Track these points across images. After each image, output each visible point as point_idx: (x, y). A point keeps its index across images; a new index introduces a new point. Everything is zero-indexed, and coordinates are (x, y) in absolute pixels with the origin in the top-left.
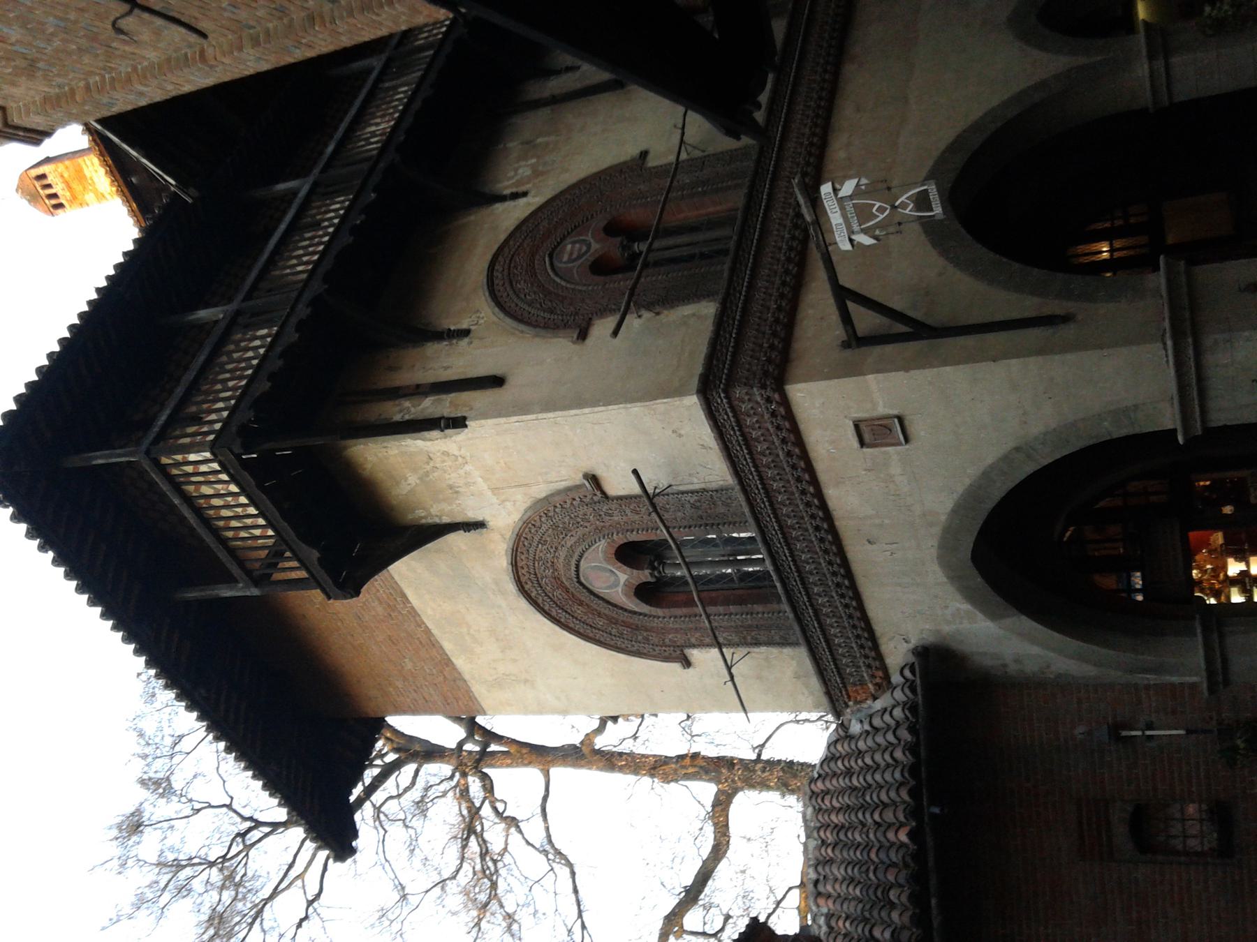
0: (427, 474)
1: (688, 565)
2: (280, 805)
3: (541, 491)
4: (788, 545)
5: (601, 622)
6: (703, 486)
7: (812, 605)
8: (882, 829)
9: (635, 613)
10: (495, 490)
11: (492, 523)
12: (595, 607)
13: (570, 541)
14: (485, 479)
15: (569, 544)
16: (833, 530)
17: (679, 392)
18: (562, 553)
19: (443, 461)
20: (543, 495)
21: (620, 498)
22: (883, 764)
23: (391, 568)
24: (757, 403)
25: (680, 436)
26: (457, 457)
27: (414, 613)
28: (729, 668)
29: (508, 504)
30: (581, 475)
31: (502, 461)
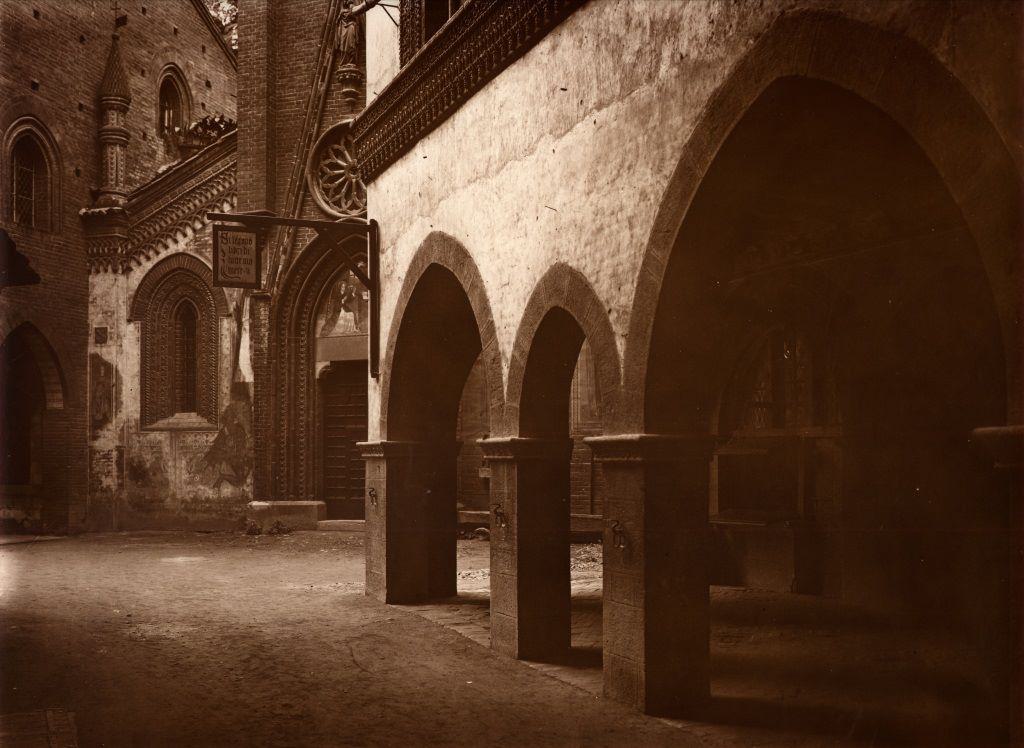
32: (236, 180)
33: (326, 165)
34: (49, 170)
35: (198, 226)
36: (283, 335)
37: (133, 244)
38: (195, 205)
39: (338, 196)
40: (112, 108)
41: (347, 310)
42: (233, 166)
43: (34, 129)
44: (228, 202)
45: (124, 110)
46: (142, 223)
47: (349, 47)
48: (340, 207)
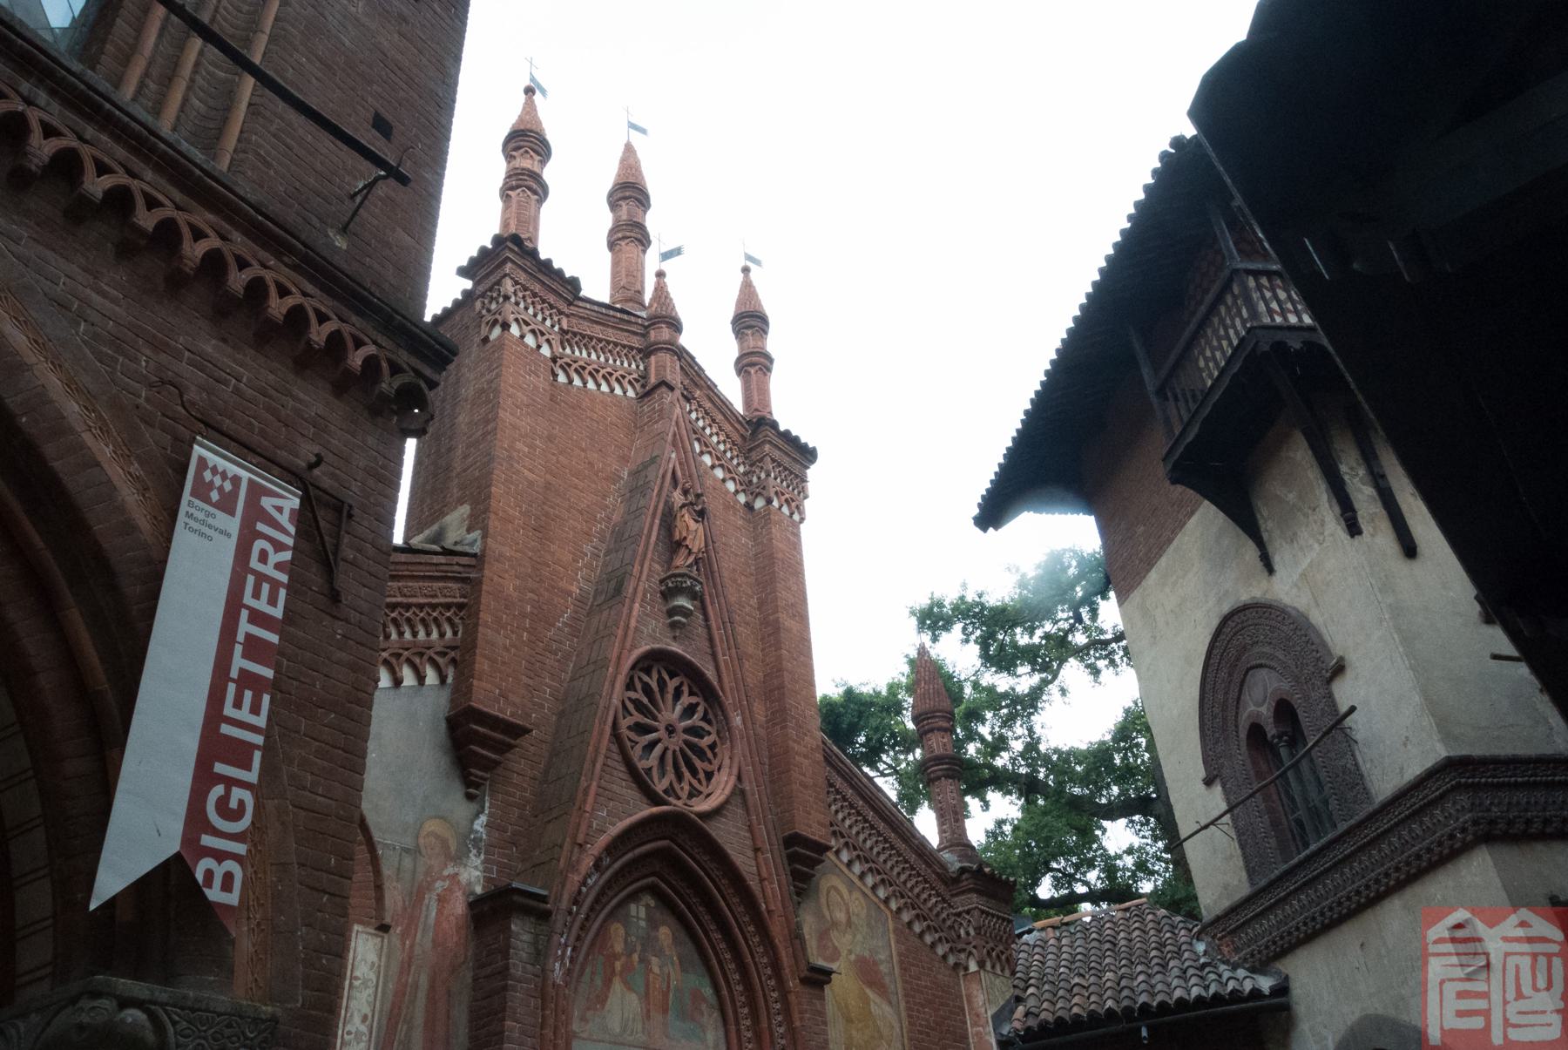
0: (1300, 510)
1: (1295, 766)
2: (1000, 465)
3: (1316, 618)
4: (1335, 865)
5: (1220, 697)
6: (1366, 774)
7: (1289, 895)
8: (1116, 987)
9: (1237, 726)
10: (1304, 576)
11: (1276, 578)
12: (1232, 688)
13: (1280, 654)
14: (1311, 565)
15: (1276, 654)
16: (1361, 909)
17: (1447, 737)
18: (1267, 649)
19: (1315, 522)
20: (1313, 622)
21: (1330, 696)
22: (1153, 982)
23: (1206, 502)
24: (1457, 819)
25: (1405, 745)
26: (1323, 533)
27: (1182, 525)
28: (1213, 823)
29: (1295, 591)
30: (1341, 654)
31: (1331, 576)
41: (629, 986)
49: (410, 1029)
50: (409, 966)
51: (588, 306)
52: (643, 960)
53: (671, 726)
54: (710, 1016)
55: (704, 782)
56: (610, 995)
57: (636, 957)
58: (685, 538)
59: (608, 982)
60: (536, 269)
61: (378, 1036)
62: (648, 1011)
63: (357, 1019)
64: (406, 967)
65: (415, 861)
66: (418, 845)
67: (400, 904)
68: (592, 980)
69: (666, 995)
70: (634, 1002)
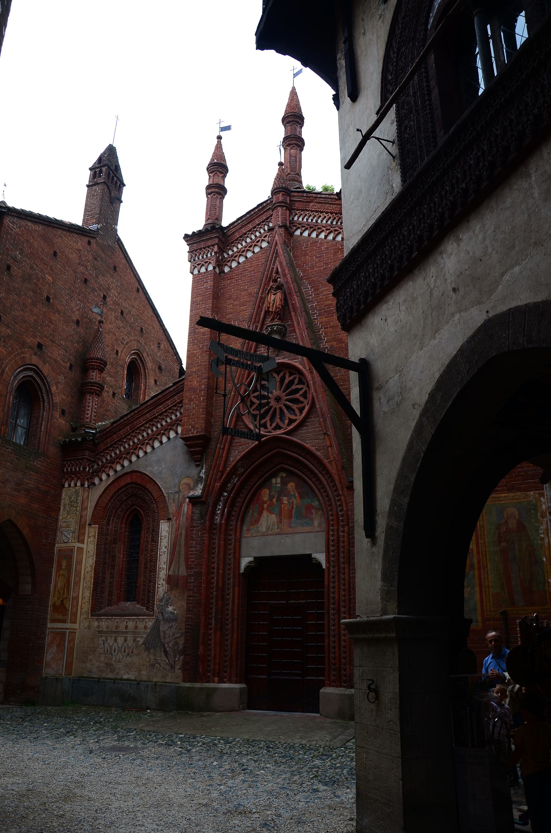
32: (181, 413)
33: (254, 397)
34: (42, 405)
35: (149, 449)
36: (214, 534)
37: (98, 465)
38: (148, 434)
39: (263, 421)
40: (94, 369)
41: (271, 512)
42: (179, 403)
43: (34, 376)
44: (173, 430)
45: (101, 371)
46: (107, 449)
47: (276, 308)
48: (266, 427)
49: (180, 547)
50: (179, 528)
51: (244, 219)
52: (279, 500)
53: (278, 397)
54: (317, 513)
55: (298, 414)
56: (261, 518)
57: (274, 500)
58: (269, 307)
59: (260, 514)
60: (199, 238)
61: (170, 551)
62: (281, 520)
63: (164, 548)
64: (177, 530)
65: (179, 495)
66: (180, 489)
67: (175, 510)
68: (253, 514)
69: (291, 511)
70: (273, 518)
